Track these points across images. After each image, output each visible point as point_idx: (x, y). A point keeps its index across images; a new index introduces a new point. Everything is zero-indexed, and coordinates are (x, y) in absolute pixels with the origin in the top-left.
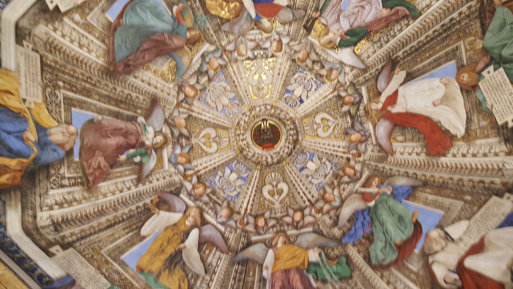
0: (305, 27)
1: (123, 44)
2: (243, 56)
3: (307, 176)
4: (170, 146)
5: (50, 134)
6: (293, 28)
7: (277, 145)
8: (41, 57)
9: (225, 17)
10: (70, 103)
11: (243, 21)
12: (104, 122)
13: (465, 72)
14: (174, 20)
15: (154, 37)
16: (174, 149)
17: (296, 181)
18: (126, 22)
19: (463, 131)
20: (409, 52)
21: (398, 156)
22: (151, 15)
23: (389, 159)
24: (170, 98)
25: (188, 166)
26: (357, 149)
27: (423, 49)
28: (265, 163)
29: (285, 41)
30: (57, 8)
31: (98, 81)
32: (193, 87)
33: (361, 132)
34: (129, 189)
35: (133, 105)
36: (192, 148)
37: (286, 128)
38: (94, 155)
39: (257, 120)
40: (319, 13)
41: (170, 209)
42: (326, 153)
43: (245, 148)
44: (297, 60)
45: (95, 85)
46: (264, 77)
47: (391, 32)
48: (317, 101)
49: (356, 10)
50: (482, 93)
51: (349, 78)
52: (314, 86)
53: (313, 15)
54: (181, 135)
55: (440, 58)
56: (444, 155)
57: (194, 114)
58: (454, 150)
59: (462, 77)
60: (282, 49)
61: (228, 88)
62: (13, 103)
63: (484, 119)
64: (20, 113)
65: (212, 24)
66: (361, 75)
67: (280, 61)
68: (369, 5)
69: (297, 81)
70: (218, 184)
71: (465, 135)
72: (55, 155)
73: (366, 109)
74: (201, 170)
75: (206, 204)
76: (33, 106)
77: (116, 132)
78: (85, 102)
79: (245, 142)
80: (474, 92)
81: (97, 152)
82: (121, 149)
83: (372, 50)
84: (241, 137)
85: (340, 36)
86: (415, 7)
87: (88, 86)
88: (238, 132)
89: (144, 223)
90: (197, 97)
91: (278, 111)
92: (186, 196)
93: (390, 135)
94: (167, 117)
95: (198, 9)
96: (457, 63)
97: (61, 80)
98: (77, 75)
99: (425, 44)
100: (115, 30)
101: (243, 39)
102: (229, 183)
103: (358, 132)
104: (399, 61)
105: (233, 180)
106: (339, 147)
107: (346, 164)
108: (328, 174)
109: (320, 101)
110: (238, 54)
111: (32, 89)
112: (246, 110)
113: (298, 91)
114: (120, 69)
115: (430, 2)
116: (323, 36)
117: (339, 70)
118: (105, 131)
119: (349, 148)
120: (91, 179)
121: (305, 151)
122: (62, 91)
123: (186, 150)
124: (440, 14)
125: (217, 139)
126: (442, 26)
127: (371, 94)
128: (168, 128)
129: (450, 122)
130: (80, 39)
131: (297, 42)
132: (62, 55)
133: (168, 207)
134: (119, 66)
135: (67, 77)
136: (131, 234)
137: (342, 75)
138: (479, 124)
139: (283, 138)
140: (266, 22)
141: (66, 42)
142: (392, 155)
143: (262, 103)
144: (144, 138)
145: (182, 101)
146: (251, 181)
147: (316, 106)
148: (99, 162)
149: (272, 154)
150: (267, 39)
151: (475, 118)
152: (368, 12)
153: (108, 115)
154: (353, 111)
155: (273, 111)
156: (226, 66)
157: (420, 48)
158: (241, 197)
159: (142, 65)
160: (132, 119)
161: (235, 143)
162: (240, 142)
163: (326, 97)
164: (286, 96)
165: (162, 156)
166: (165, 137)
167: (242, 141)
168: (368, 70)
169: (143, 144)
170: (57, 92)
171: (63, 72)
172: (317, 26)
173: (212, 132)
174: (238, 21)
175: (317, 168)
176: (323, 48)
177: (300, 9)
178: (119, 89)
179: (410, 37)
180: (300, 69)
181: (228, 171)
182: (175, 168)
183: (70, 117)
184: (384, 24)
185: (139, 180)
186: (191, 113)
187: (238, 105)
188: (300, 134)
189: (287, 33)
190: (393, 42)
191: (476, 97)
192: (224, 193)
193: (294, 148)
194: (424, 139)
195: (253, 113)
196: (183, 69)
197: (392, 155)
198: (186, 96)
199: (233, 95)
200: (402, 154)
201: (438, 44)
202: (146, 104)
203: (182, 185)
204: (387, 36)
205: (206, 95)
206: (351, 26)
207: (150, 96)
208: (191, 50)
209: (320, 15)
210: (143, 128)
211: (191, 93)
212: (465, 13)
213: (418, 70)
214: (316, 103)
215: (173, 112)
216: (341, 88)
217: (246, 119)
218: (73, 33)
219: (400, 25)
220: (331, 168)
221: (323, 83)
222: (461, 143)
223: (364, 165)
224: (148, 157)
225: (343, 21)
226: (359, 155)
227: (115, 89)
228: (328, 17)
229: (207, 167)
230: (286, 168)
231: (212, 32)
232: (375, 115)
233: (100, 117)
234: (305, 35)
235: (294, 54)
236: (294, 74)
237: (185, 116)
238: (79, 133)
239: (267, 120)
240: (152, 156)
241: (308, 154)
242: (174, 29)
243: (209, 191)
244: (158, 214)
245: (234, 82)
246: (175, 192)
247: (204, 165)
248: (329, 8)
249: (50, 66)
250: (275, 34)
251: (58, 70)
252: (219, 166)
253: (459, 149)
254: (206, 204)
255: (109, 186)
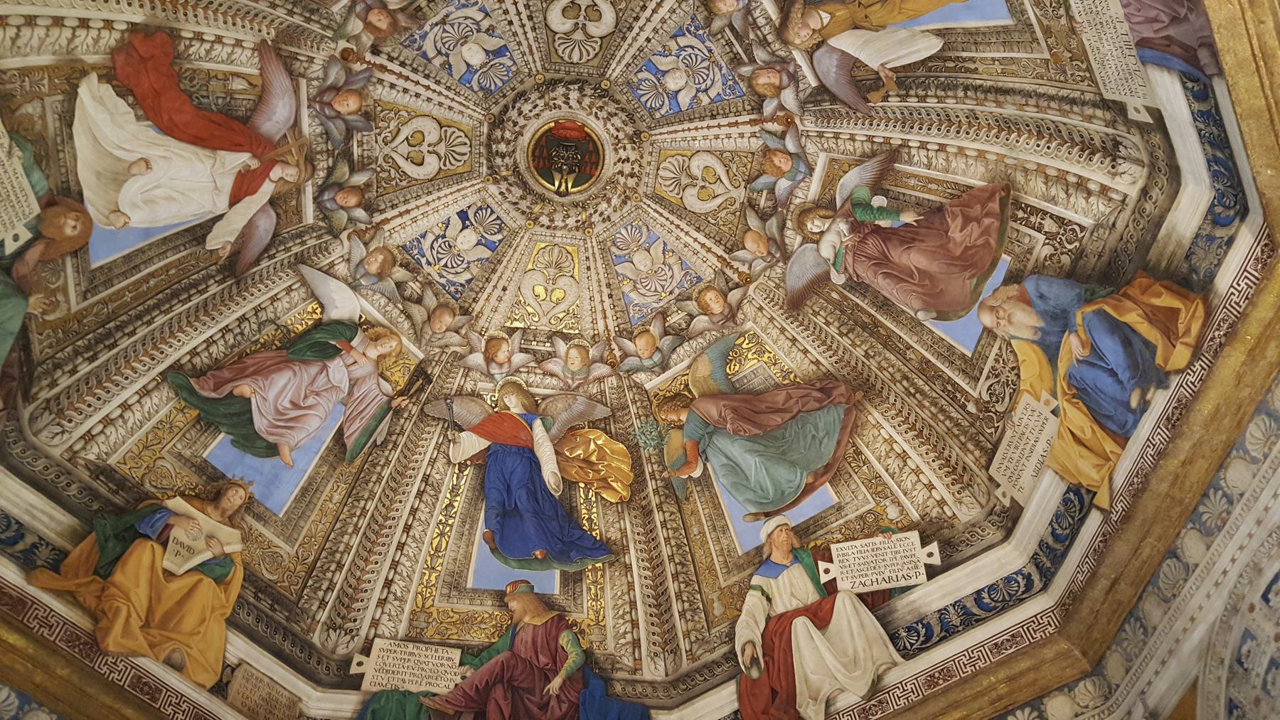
0: (428, 379)
1: (821, 434)
2: (576, 346)
3: (490, 31)
4: (797, 201)
5: (1036, 329)
6: (457, 381)
7: (546, 127)
8: (987, 468)
9: (599, 432)
10: (971, 367)
11: (564, 416)
12: (917, 304)
13: (70, 238)
14: (704, 451)
15: (756, 431)
16: (791, 193)
17: (523, 26)
18: (802, 474)
19: (83, 91)
20: (194, 291)
21: (250, 39)
22: (747, 472)
23: (273, 33)
24: (760, 301)
25: (773, 143)
26: (349, 72)
27: (160, 296)
28: (588, 91)
29: (477, 359)
30: (925, 542)
31: (894, 381)
32: (705, 311)
33: (333, 114)
34: (923, 146)
35: (843, 312)
36: (750, 180)
37: (515, 162)
38: (967, 248)
39: (578, 198)
40: (395, 404)
41: (851, 65)
42: (427, 77)
43: (626, 142)
44: (458, 312)
45: (906, 378)
46: (540, 290)
47: (232, 341)
48: (427, 208)
49: (311, 401)
50: (33, 187)
51: (340, 248)
52: (426, 244)
53: (406, 402)
54: (764, 217)
55: (125, 275)
56: (133, 27)
57: (720, 252)
58: (110, 39)
59: (78, 228)
60: (488, 342)
61: (627, 288)
62: (1078, 419)
63: (30, 117)
64: (1074, 396)
65: (627, 424)
66: (311, 251)
67: (498, 319)
68: (280, 408)
69: (465, 266)
70: (718, 76)
71: (79, 79)
72: (1044, 289)
73: (309, 168)
74: (743, 123)
75: (764, 43)
76: (1045, 395)
77: (901, 276)
78: (939, 356)
79: (623, 154)
80: (50, 190)
81: (958, 253)
82: (906, 236)
83: (281, 306)
84: (627, 168)
85: (352, 348)
86: (177, 394)
87: (920, 383)
88: (631, 182)
89: (923, 62)
90: (702, 285)
91: (524, 205)
92: (805, 77)
93: (261, 95)
94: (781, 264)
95: (649, 459)
96: (87, 262)
97: (969, 413)
98: (933, 409)
99: (157, 306)
100: (828, 467)
101: (570, 382)
102: (691, 71)
103: (339, 115)
104: (219, 272)
105: (678, 74)
106: (392, 86)
107: (385, 40)
108: (437, 24)
109: (418, 207)
110: (588, 351)
111: (1031, 424)
112: (599, 228)
113: (466, 241)
114: (842, 389)
115: (143, 401)
116: (390, 354)
117: (362, 271)
118: (922, 286)
119: (368, 80)
120: (995, 206)
121: (481, 94)
122: (976, 395)
123: (764, 180)
124: (119, 372)
125: (685, 178)
126: (114, 345)
127: (294, 203)
128: (787, 241)
129: (111, 114)
130: (901, 470)
131: (449, 351)
132: (946, 453)
133: (856, 72)
134: (842, 395)
135: (954, 415)
136: (964, 54)
137: (356, 258)
138: (43, 107)
139: (525, 139)
140: (514, 405)
141: (929, 475)
142: (264, 41)
143: (559, 233)
144: (848, 239)
145: (737, 286)
146: (634, 57)
147: (430, 198)
148: (961, 231)
149: (563, 105)
150: (517, 371)
151: (52, 123)
152: (284, 394)
153: (903, 311)
154: (344, 169)
155: (537, 209)
156: (620, 334)
157: (168, 299)
158: (671, 26)
159: (794, 384)
160: (855, 285)
161: (647, 158)
162: (632, 158)
163: (401, 215)
164: (499, 237)
165: (824, 187)
166: (800, 226)
167: (628, 160)
168: (292, 259)
169: (855, 227)
170: (986, 397)
171: (958, 425)
172: (401, 378)
173: (691, 199)
174: (572, 420)
175: (462, 45)
176: (393, 328)
177: (434, 419)
178: (859, 352)
179: (189, 324)
180: (452, 289)
181: (684, 99)
182: (803, 148)
183: (982, 342)
184: (249, 361)
185: (893, 154)
186: (726, 256)
187: (614, 244)
188: (484, 138)
189: (470, 374)
190: (230, 318)
191: (48, 177)
192: (710, 51)
193: (506, 109)
194: (179, 77)
195: (584, 216)
196: (714, 352)
197: (264, 41)
198: (725, 296)
199: (619, 268)
200: (238, 43)
201: (127, 304)
202: (815, 303)
203: (803, 104)
204: (242, 334)
205: (680, 285)
206: (325, 367)
207: (800, 318)
208: (687, 386)
209: (392, 398)
210: (839, 260)
211: (710, 297)
212: (64, 373)
213: (176, 249)
214: (428, 203)
215: (764, 270)
216: (363, 227)
217: (604, 205)
218: (910, 486)
219: (210, 354)
220: (424, 37)
221: (404, 247)
222: (91, 59)
223: (340, 26)
224: (855, 196)
225: (341, 383)
226: (346, 54)
227: (867, 356)
228: (374, 392)
229: (730, 125)
230: (539, 64)
231: (633, 409)
232: (290, 151)
233: (921, 315)
234: (431, 361)
235: (461, 327)
236: (469, 281)
237: (740, 254)
238: (977, 304)
239: (558, 193)
240: (845, 196)
241: (476, 88)
242: (711, 434)
243: (746, 70)
244: (882, 65)
245: (610, 296)
246: (827, 98)
247: (734, 131)
248: (371, 411)
249: (978, 445)
250: (498, 377)
251: (965, 433)
252: (702, 118)
253: (96, 41)
254: (764, 43)
255: (964, 174)
